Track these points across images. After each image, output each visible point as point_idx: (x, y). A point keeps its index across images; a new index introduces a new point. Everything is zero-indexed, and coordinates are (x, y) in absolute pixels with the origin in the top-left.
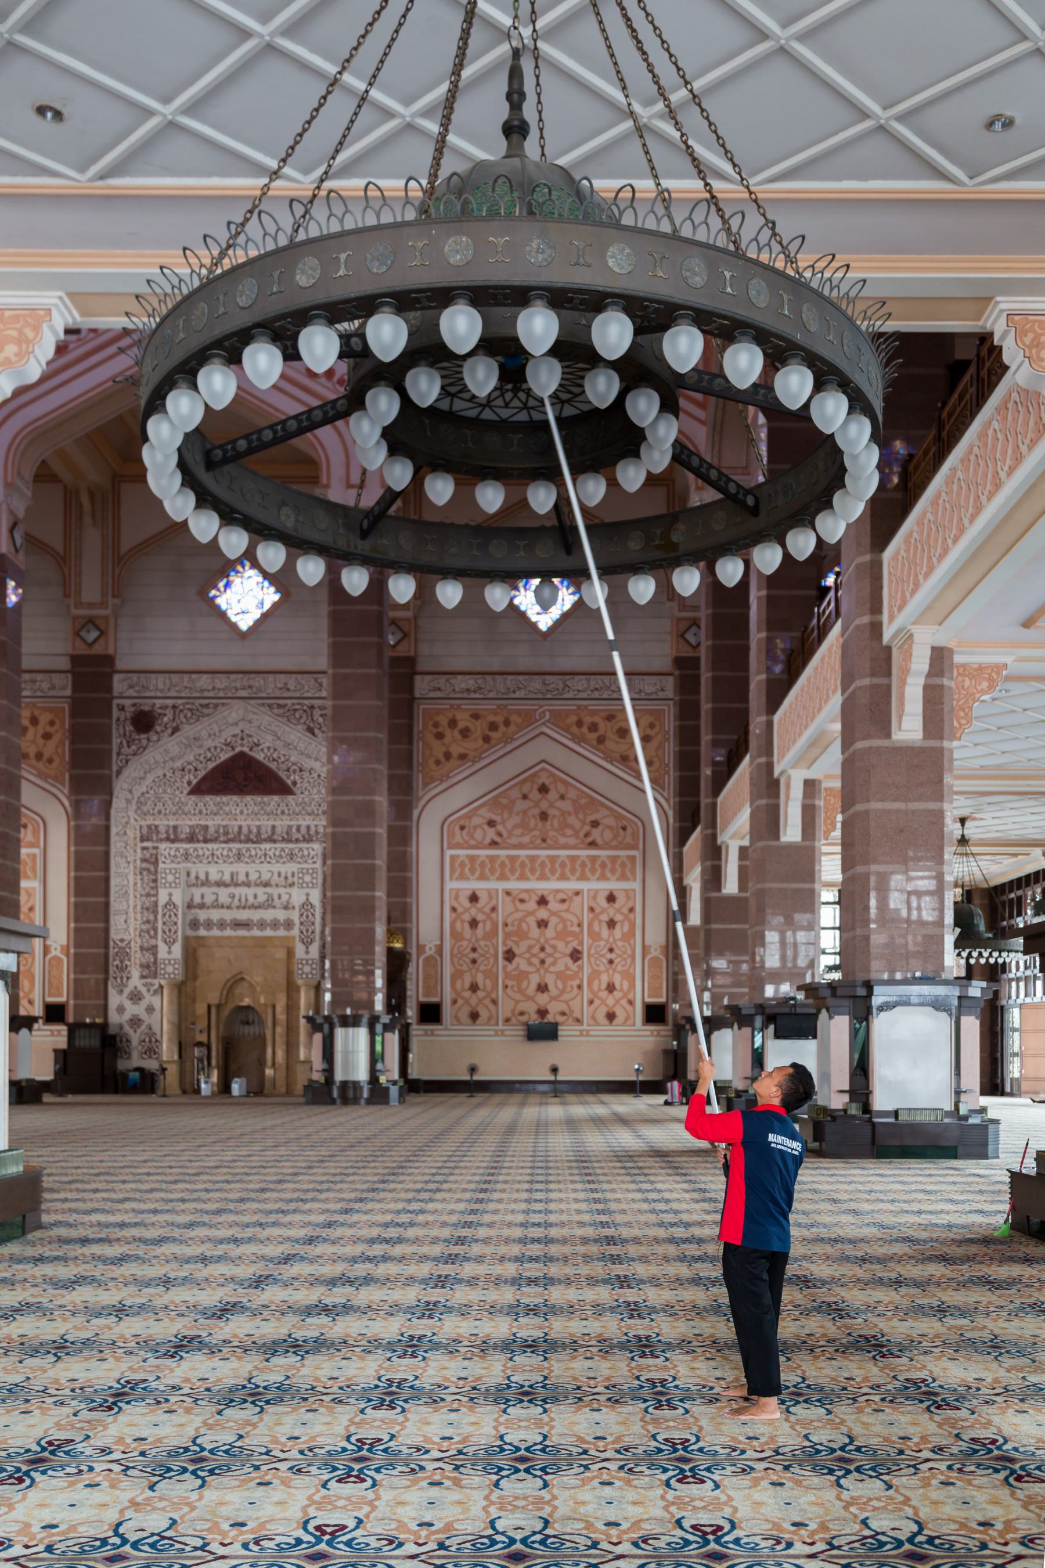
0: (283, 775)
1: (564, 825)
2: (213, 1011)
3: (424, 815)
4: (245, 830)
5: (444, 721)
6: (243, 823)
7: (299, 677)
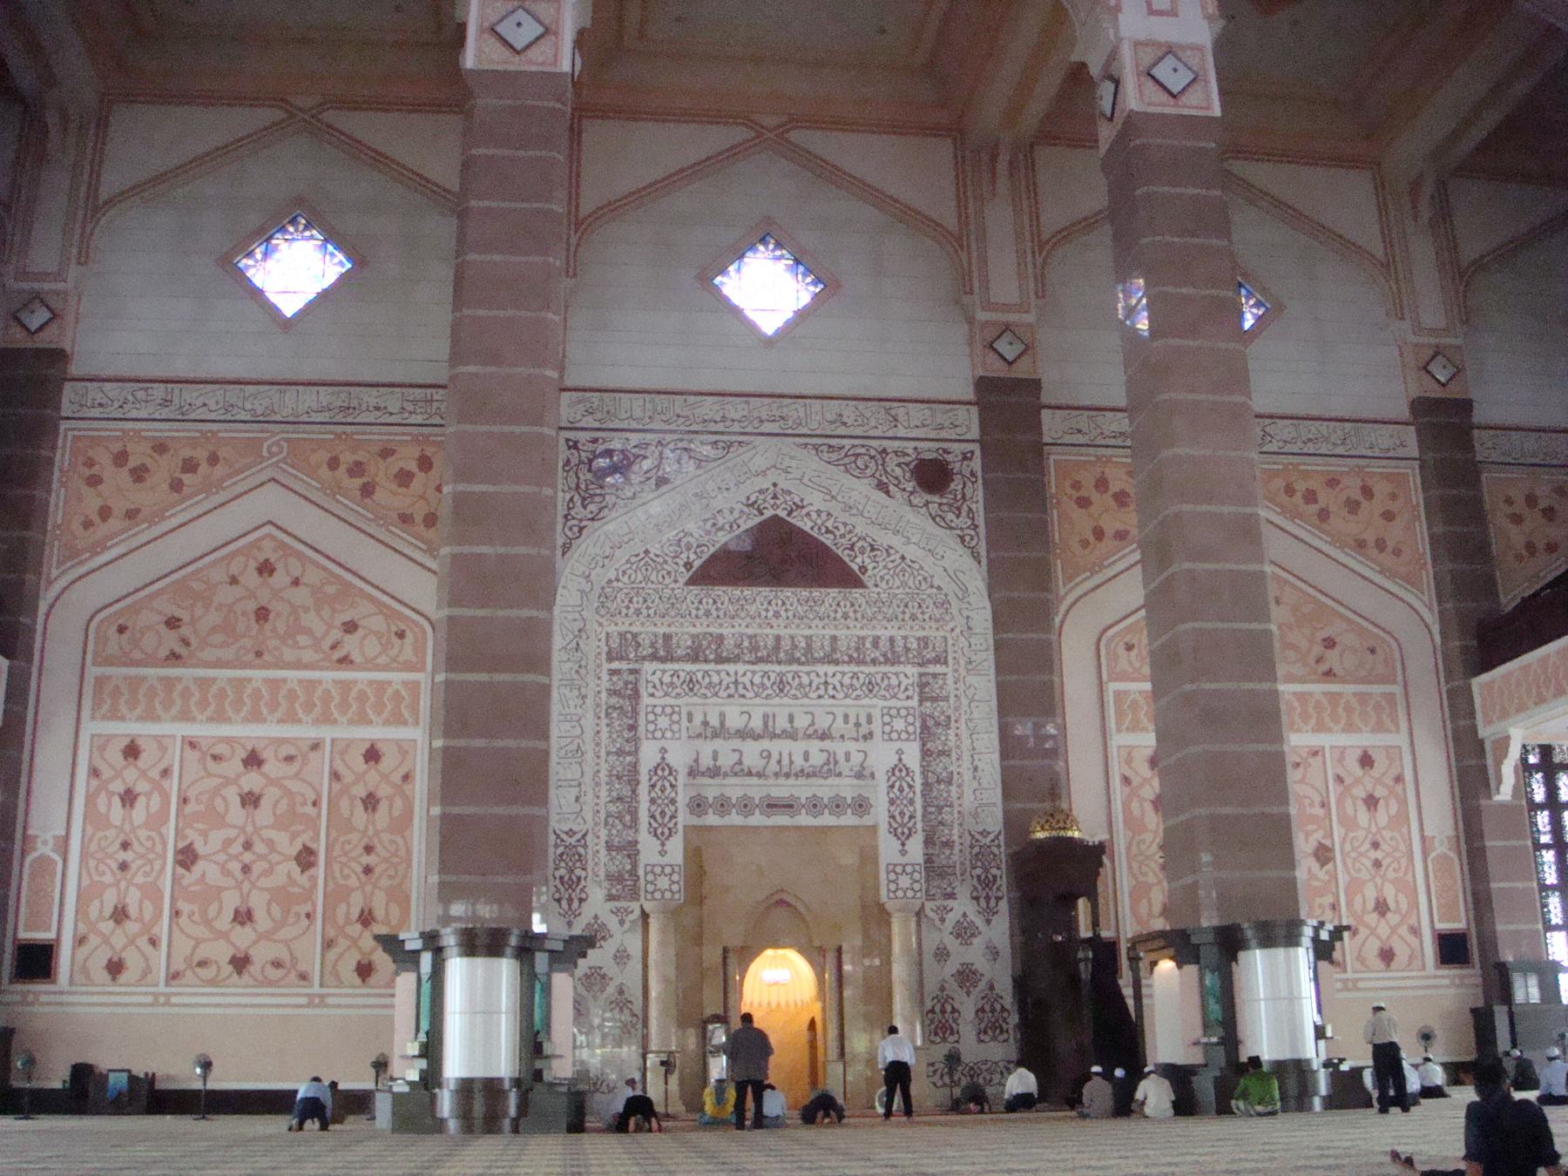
2: (732, 960)
3: (1067, 622)
5: (1087, 479)
6: (783, 632)
7: (861, 405)
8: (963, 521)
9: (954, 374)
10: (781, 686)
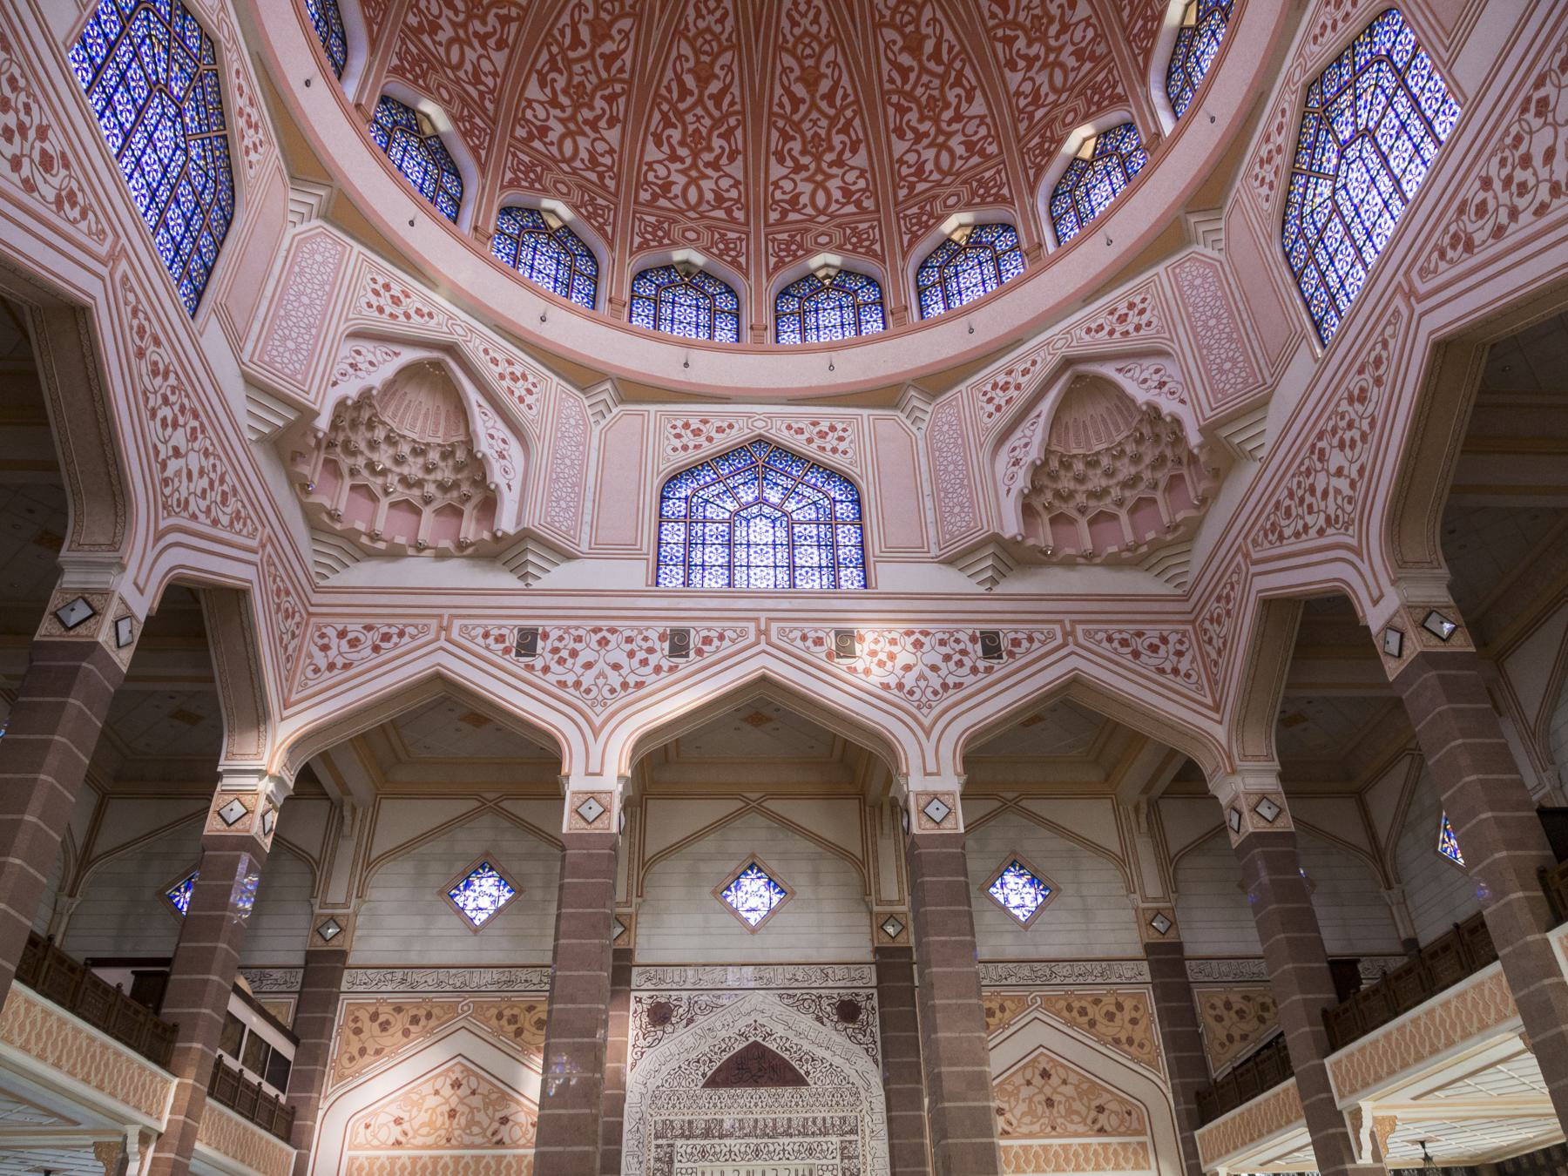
0: (796, 1065)
1: (1070, 1112)
4: (761, 1124)
8: (868, 1039)
9: (860, 947)
10: (757, 1152)
